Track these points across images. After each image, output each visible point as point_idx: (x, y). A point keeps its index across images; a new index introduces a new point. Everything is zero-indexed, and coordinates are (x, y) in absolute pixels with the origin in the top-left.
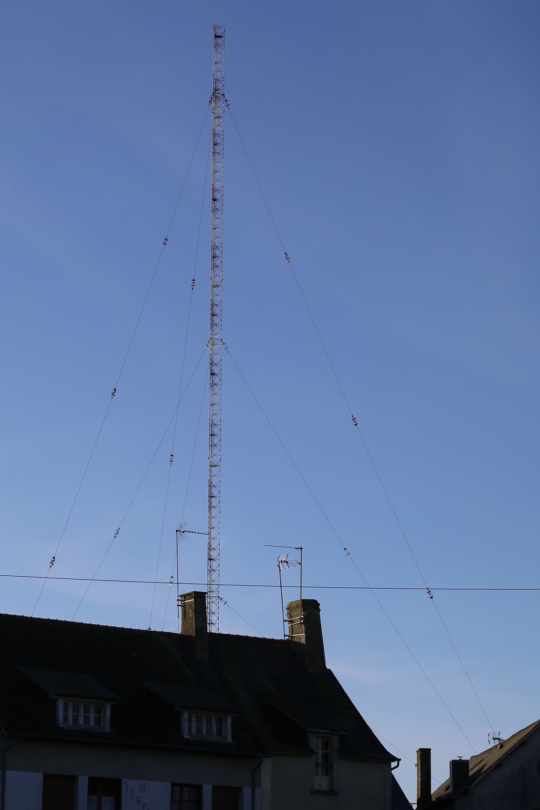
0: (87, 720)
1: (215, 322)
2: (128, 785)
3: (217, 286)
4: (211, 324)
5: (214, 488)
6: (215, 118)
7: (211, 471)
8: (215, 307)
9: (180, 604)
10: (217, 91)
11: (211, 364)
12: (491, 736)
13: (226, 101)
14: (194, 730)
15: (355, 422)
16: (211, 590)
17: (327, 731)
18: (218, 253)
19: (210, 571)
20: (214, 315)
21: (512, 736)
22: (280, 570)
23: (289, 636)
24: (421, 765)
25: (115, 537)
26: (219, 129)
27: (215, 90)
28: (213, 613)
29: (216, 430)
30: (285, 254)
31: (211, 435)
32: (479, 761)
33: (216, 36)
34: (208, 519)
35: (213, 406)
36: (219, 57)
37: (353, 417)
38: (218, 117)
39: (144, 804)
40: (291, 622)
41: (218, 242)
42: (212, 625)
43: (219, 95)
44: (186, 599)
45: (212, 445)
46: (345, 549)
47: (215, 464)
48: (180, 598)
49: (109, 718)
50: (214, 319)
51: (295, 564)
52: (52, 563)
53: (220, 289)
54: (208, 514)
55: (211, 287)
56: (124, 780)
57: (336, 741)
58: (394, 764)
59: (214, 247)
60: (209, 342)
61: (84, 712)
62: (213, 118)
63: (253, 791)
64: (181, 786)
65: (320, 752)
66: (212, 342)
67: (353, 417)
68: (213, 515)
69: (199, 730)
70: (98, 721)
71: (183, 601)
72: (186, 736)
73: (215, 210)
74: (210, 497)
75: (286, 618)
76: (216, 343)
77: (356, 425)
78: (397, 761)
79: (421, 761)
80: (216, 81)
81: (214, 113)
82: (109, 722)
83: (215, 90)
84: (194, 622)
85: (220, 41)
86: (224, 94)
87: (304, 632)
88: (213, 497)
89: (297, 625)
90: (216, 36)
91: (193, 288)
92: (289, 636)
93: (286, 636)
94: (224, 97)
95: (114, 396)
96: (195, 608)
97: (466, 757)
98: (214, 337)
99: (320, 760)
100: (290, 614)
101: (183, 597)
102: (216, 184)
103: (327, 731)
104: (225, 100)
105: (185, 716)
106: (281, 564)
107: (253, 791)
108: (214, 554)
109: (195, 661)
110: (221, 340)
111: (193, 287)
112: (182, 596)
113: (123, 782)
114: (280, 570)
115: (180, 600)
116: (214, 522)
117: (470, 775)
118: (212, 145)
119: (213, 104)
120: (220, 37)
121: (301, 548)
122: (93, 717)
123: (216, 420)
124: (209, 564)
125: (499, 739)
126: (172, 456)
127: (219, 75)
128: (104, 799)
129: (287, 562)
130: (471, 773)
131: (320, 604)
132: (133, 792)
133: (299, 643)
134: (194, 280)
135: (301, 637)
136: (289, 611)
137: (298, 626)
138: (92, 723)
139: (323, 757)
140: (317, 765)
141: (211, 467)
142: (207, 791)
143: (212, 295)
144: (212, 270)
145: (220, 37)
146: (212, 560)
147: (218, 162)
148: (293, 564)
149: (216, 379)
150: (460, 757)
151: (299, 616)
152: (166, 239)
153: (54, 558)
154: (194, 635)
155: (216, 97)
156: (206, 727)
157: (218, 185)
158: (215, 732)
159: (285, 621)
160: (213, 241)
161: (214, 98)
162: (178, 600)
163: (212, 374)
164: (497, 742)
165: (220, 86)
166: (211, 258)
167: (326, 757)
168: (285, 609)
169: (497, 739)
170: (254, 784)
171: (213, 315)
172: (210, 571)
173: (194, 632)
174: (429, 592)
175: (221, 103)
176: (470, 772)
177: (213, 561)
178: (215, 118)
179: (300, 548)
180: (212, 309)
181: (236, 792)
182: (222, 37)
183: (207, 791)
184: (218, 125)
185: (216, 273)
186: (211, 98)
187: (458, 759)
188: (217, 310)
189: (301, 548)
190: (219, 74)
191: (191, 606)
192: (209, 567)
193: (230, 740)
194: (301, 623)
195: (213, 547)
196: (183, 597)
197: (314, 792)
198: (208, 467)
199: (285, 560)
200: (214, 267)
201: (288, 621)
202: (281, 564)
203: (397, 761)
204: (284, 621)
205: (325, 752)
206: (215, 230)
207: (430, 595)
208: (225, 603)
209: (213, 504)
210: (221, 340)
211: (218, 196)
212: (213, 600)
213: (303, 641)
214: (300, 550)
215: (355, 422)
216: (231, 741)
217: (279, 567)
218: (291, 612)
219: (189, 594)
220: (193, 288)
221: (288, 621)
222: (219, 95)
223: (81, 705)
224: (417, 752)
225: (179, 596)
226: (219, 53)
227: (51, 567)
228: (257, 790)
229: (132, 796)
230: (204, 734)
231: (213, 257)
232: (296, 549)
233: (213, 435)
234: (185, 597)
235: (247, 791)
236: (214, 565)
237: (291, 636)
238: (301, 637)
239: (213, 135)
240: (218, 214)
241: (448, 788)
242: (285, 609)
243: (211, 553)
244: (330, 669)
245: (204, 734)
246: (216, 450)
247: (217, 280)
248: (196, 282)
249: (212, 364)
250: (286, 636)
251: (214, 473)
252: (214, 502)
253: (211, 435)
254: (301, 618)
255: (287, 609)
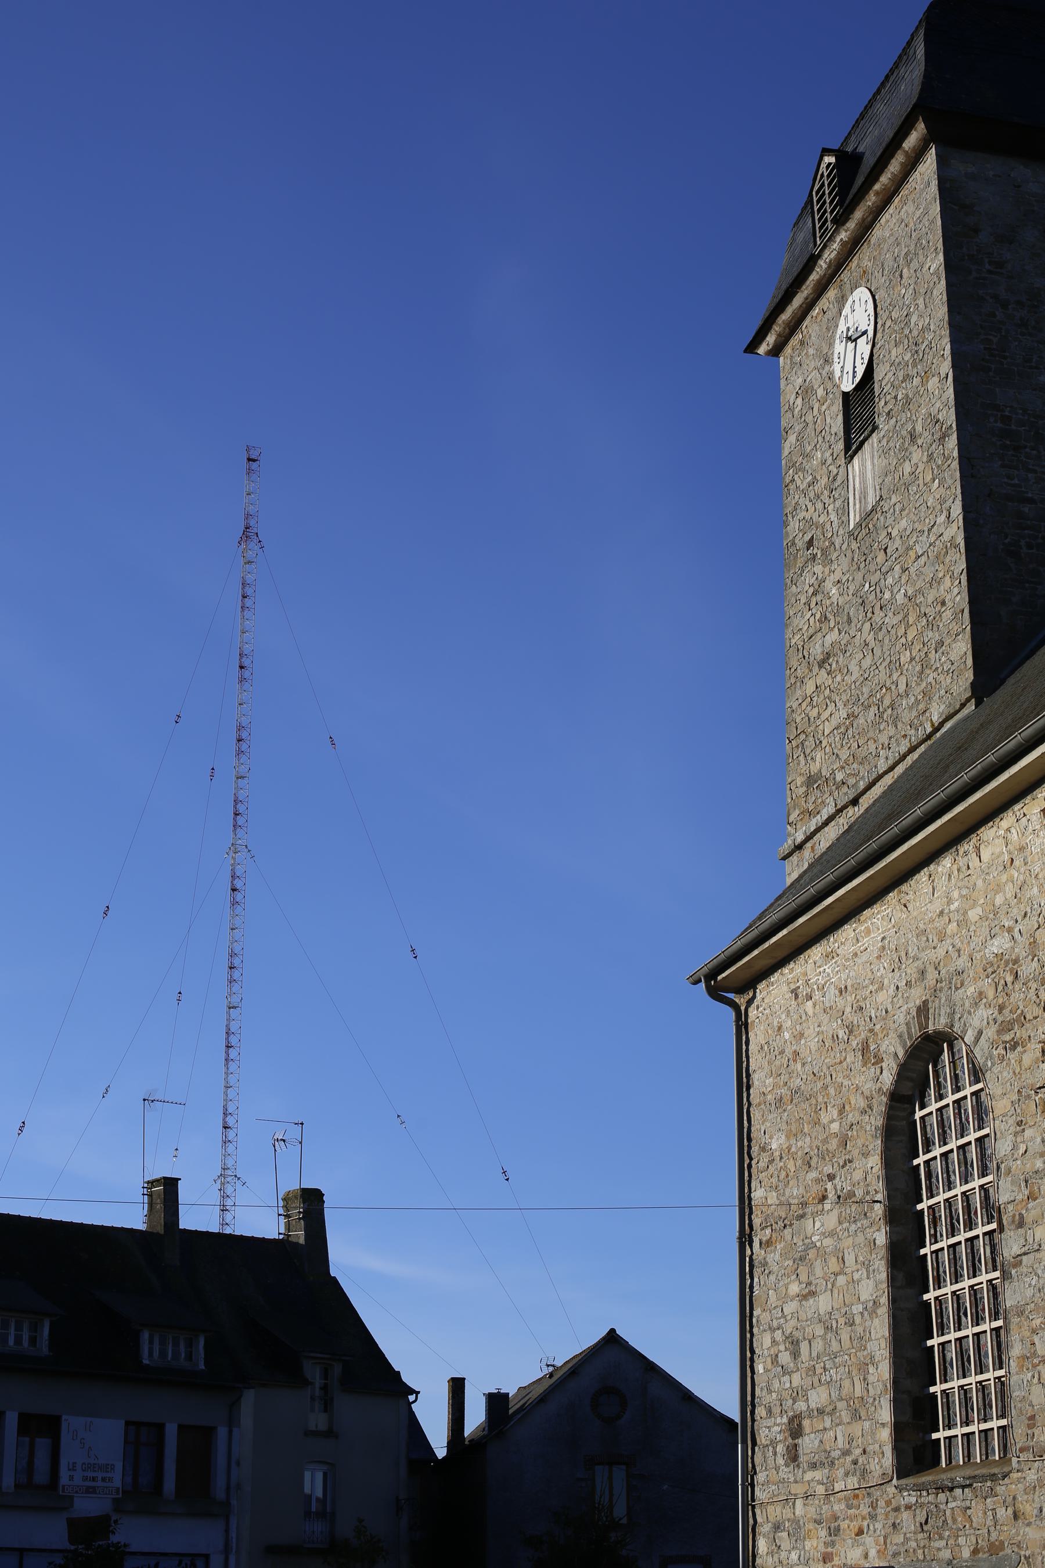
0: (18, 1340)
1: (239, 823)
2: (69, 1424)
3: (242, 777)
4: (234, 826)
5: (232, 1036)
6: (245, 563)
7: (228, 1013)
8: (239, 805)
9: (146, 1193)
10: (249, 529)
11: (232, 877)
12: (544, 1362)
13: (260, 541)
14: (156, 1354)
15: (414, 954)
16: (226, 1167)
17: (326, 1356)
18: (244, 735)
19: (225, 1142)
20: (238, 815)
21: (564, 1363)
22: (275, 1150)
23: (284, 1234)
24: (452, 1399)
25: (103, 1097)
26: (250, 578)
27: (246, 528)
28: (228, 1196)
29: (237, 962)
30: (331, 738)
31: (231, 968)
32: (527, 1392)
33: (249, 460)
34: (224, 1076)
35: (234, 931)
36: (253, 486)
37: (411, 947)
38: (249, 562)
39: (90, 1447)
40: (287, 1216)
41: (244, 721)
42: (227, 1212)
43: (250, 534)
44: (154, 1186)
45: (231, 981)
46: (398, 1116)
47: (235, 1004)
48: (146, 1185)
49: (47, 1338)
50: (238, 819)
51: (294, 1144)
52: (21, 1130)
53: (246, 781)
54: (224, 1069)
55: (234, 779)
56: (64, 1417)
57: (337, 1369)
58: (412, 1398)
59: (240, 728)
60: (230, 848)
61: (16, 1330)
62: (242, 563)
63: (230, 1432)
64: (138, 1424)
65: (318, 1382)
66: (234, 848)
67: (411, 947)
68: (231, 1070)
69: (163, 1353)
70: (33, 1341)
71: (149, 1188)
72: (146, 1362)
73: (242, 680)
74: (228, 1047)
75: (281, 1211)
76: (239, 850)
77: (415, 957)
78: (414, 1395)
79: (452, 1393)
80: (248, 516)
81: (244, 557)
82: (47, 1342)
83: (246, 528)
84: (163, 1216)
85: (254, 465)
86: (257, 533)
87: (303, 1230)
88: (230, 1047)
89: (294, 1221)
90: (249, 460)
91: (211, 779)
92: (284, 1234)
93: (281, 1234)
94: (257, 536)
95: (107, 915)
96: (164, 1197)
97: (511, 1389)
98: (238, 843)
99: (317, 1392)
100: (286, 1207)
101: (150, 1184)
102: (244, 647)
103: (326, 1356)
104: (258, 541)
105: (146, 1335)
106: (276, 1143)
107: (230, 1432)
108: (230, 1121)
109: (163, 1264)
110: (246, 846)
111: (212, 777)
112: (148, 1182)
113: (63, 1419)
114: (275, 1150)
115: (145, 1188)
116: (232, 1080)
117: (510, 1413)
118: (240, 597)
119: (243, 546)
120: (254, 460)
121: (302, 1124)
122: (27, 1336)
123: (237, 949)
124: (224, 1134)
125: (553, 1366)
126: (180, 993)
127: (251, 509)
128: (39, 1441)
129: (284, 1141)
130: (511, 1412)
131: (324, 1195)
132: (75, 1433)
133: (297, 1244)
134: (213, 769)
135: (299, 1235)
136: (285, 1202)
137: (296, 1222)
138: (26, 1343)
139: (321, 1388)
140: (313, 1399)
141: (230, 1008)
142: (171, 1431)
143: (235, 788)
144: (237, 757)
145: (254, 460)
146: (228, 1128)
147: (247, 619)
148: (292, 1143)
149: (239, 897)
150: (499, 1389)
151: (297, 1210)
152: (179, 716)
153: (23, 1123)
154: (162, 1232)
155: (247, 537)
156: (172, 1350)
157: (247, 648)
158: (183, 1355)
159: (281, 1215)
160: (239, 720)
161: (244, 538)
162: (143, 1187)
163: (234, 890)
164: (551, 1369)
165: (252, 523)
166: (235, 741)
167: (325, 1388)
168: (280, 1199)
169: (551, 1365)
170: (232, 1422)
171: (236, 814)
172: (225, 1142)
173: (163, 1228)
174: (504, 1172)
175: (253, 544)
176: (510, 1411)
177: (229, 1130)
178: (245, 563)
179: (300, 1124)
180: (235, 807)
181: (209, 1432)
182: (257, 460)
183: (171, 1431)
184: (249, 573)
185: (242, 761)
186: (241, 538)
187: (496, 1391)
188: (241, 808)
189: (302, 1124)
190: (252, 507)
191: (160, 1195)
192: (224, 1137)
193: (202, 1367)
194: (299, 1219)
195: (230, 1110)
196: (150, 1184)
197: (308, 1433)
198: (226, 1009)
199: (281, 1138)
200: (239, 753)
201: (284, 1215)
202: (276, 1143)
203: (414, 1395)
204: (279, 1215)
205: (325, 1383)
206: (242, 706)
207: (506, 1176)
208: (244, 1184)
209: (231, 1056)
210: (246, 846)
211: (246, 662)
212: (229, 1179)
213: (302, 1241)
214: (301, 1125)
215: (414, 954)
216: (203, 1368)
217: (274, 1147)
218: (287, 1203)
219: (157, 1180)
220: (211, 779)
221: (284, 1215)
222: (250, 534)
223: (12, 1321)
224: (448, 1382)
225: (144, 1183)
226: (253, 481)
227: (19, 1134)
228: (235, 1430)
229: (75, 1438)
230: (169, 1359)
231: (239, 741)
232: (296, 1124)
233: (233, 968)
234: (152, 1183)
235: (222, 1432)
236: (231, 1134)
237: (287, 1235)
238: (299, 1235)
239: (242, 584)
240: (246, 685)
241: (484, 1429)
242: (280, 1199)
243: (227, 1119)
244: (335, 1277)
245: (169, 1359)
246: (236, 987)
247: (243, 770)
248: (216, 771)
249: (234, 877)
250: (281, 1234)
251: (233, 1016)
252: (233, 1053)
253: (231, 968)
254: (300, 1212)
255: (282, 1199)
